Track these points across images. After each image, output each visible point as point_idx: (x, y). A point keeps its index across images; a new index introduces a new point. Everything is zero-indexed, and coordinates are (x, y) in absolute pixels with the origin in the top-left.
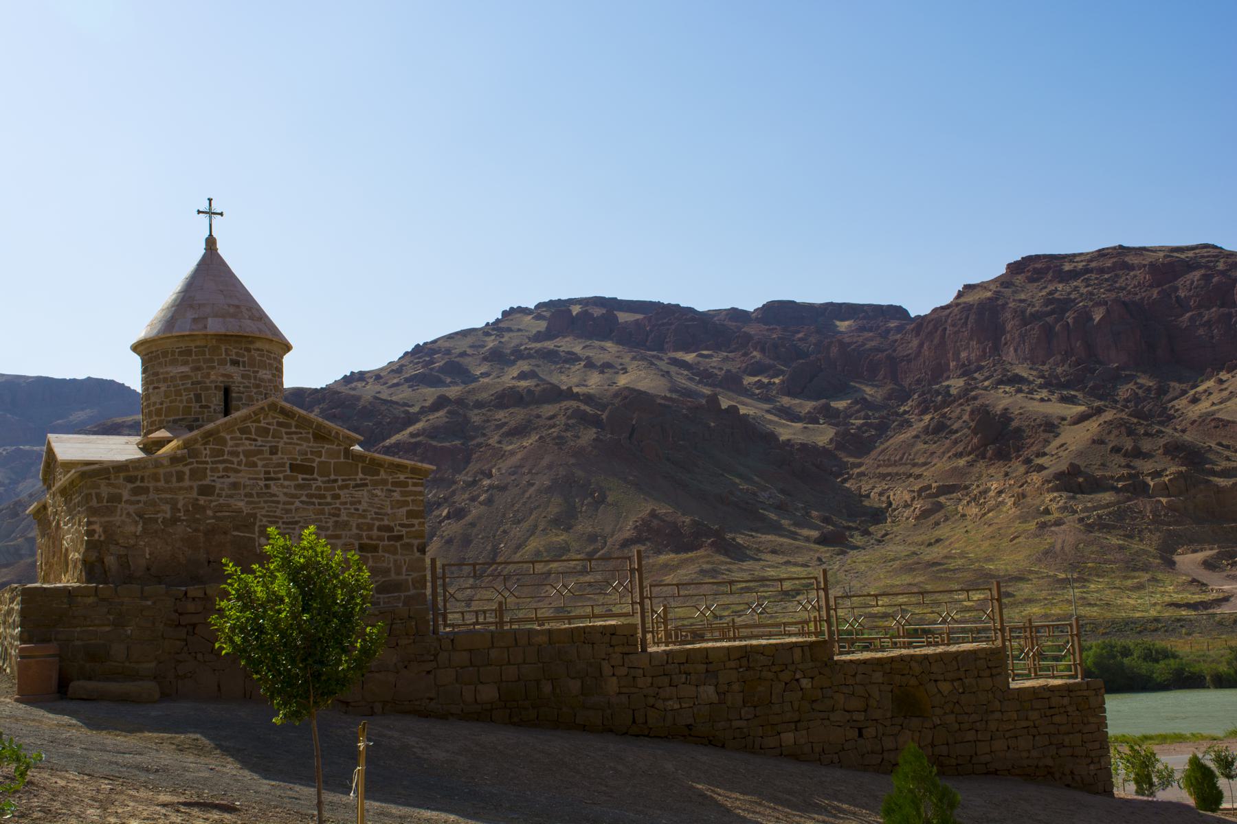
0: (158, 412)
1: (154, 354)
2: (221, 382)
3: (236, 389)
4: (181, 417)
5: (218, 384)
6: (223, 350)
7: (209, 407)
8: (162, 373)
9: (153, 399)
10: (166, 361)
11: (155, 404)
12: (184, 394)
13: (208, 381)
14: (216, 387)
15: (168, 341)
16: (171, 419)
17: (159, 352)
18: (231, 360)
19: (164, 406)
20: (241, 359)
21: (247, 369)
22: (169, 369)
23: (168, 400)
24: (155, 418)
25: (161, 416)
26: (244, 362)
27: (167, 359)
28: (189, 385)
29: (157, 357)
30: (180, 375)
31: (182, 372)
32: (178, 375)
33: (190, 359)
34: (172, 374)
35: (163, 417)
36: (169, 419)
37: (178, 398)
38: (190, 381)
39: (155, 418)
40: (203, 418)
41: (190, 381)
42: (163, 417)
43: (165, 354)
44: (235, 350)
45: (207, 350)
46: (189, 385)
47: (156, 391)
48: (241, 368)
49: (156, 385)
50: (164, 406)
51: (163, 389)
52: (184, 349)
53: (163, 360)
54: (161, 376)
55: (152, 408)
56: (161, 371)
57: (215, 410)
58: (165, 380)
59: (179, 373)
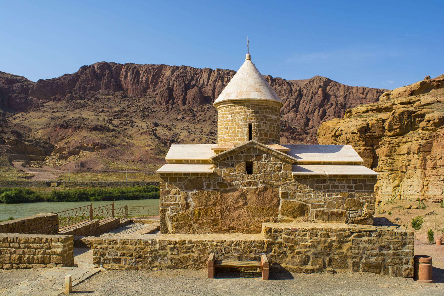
0: (266, 135)
1: (264, 107)
8: (268, 117)
9: (263, 128)
11: (264, 130)
15: (272, 103)
16: (272, 139)
17: (267, 106)
19: (269, 132)
22: (271, 116)
23: (270, 130)
24: (264, 137)
25: (267, 137)
29: (265, 108)
34: (272, 119)
35: (268, 138)
36: (270, 139)
39: (264, 137)
42: (268, 138)
43: (269, 108)
47: (265, 124)
50: (269, 132)
51: (269, 124)
53: (269, 111)
55: (262, 132)
56: (268, 116)
58: (269, 120)
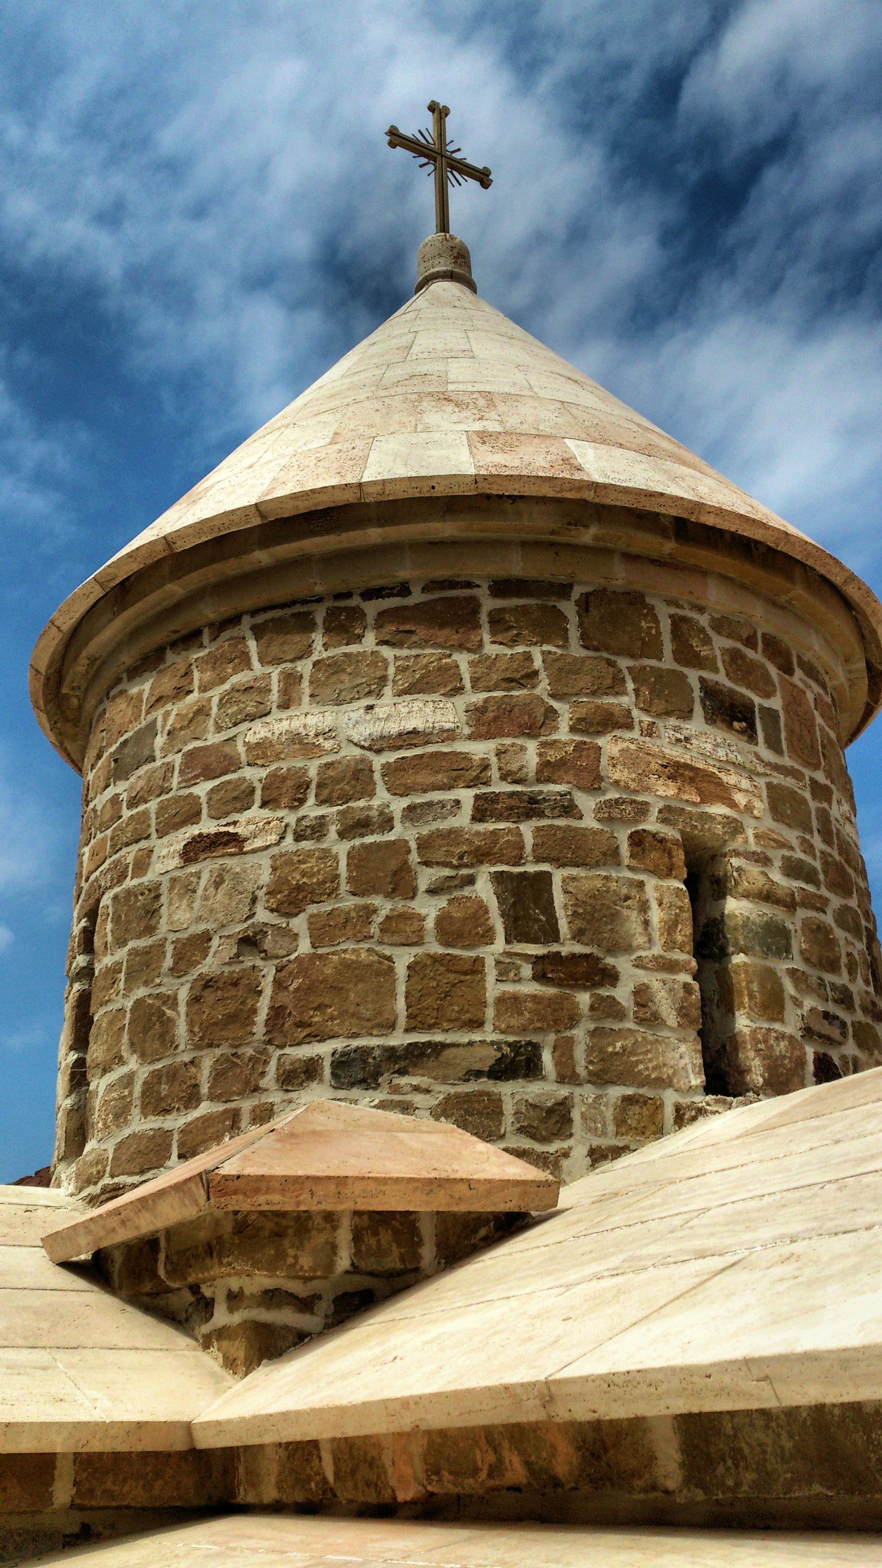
2: (668, 814)
3: (753, 870)
4: (399, 1039)
5: (651, 825)
6: (666, 626)
7: (611, 977)
10: (291, 680)
12: (426, 877)
13: (586, 803)
14: (638, 840)
18: (710, 692)
20: (757, 700)
21: (787, 761)
26: (770, 715)
27: (305, 667)
28: (463, 820)
30: (391, 757)
31: (410, 737)
32: (378, 761)
33: (463, 660)
37: (384, 906)
38: (466, 796)
40: (563, 1050)
41: (466, 796)
44: (721, 643)
45: (569, 608)
46: (463, 820)
48: (767, 755)
49: (208, 826)
52: (417, 597)
53: (275, 673)
54: (254, 775)
56: (257, 732)
57: (642, 995)
59: (379, 745)
